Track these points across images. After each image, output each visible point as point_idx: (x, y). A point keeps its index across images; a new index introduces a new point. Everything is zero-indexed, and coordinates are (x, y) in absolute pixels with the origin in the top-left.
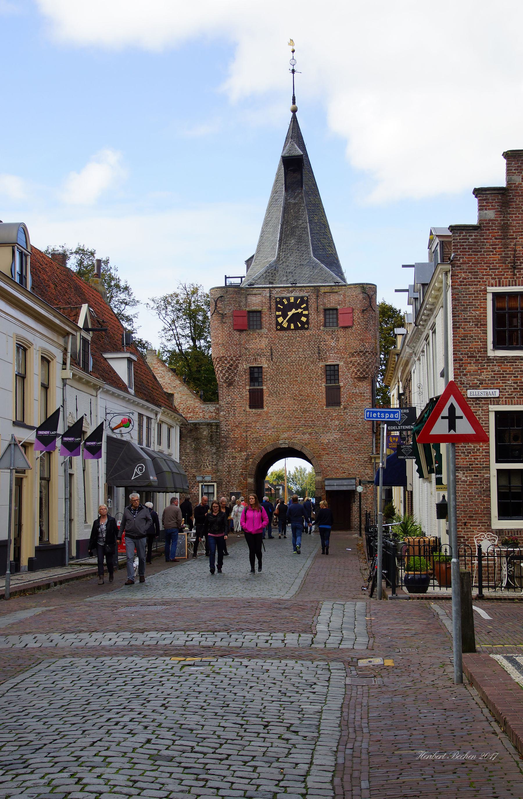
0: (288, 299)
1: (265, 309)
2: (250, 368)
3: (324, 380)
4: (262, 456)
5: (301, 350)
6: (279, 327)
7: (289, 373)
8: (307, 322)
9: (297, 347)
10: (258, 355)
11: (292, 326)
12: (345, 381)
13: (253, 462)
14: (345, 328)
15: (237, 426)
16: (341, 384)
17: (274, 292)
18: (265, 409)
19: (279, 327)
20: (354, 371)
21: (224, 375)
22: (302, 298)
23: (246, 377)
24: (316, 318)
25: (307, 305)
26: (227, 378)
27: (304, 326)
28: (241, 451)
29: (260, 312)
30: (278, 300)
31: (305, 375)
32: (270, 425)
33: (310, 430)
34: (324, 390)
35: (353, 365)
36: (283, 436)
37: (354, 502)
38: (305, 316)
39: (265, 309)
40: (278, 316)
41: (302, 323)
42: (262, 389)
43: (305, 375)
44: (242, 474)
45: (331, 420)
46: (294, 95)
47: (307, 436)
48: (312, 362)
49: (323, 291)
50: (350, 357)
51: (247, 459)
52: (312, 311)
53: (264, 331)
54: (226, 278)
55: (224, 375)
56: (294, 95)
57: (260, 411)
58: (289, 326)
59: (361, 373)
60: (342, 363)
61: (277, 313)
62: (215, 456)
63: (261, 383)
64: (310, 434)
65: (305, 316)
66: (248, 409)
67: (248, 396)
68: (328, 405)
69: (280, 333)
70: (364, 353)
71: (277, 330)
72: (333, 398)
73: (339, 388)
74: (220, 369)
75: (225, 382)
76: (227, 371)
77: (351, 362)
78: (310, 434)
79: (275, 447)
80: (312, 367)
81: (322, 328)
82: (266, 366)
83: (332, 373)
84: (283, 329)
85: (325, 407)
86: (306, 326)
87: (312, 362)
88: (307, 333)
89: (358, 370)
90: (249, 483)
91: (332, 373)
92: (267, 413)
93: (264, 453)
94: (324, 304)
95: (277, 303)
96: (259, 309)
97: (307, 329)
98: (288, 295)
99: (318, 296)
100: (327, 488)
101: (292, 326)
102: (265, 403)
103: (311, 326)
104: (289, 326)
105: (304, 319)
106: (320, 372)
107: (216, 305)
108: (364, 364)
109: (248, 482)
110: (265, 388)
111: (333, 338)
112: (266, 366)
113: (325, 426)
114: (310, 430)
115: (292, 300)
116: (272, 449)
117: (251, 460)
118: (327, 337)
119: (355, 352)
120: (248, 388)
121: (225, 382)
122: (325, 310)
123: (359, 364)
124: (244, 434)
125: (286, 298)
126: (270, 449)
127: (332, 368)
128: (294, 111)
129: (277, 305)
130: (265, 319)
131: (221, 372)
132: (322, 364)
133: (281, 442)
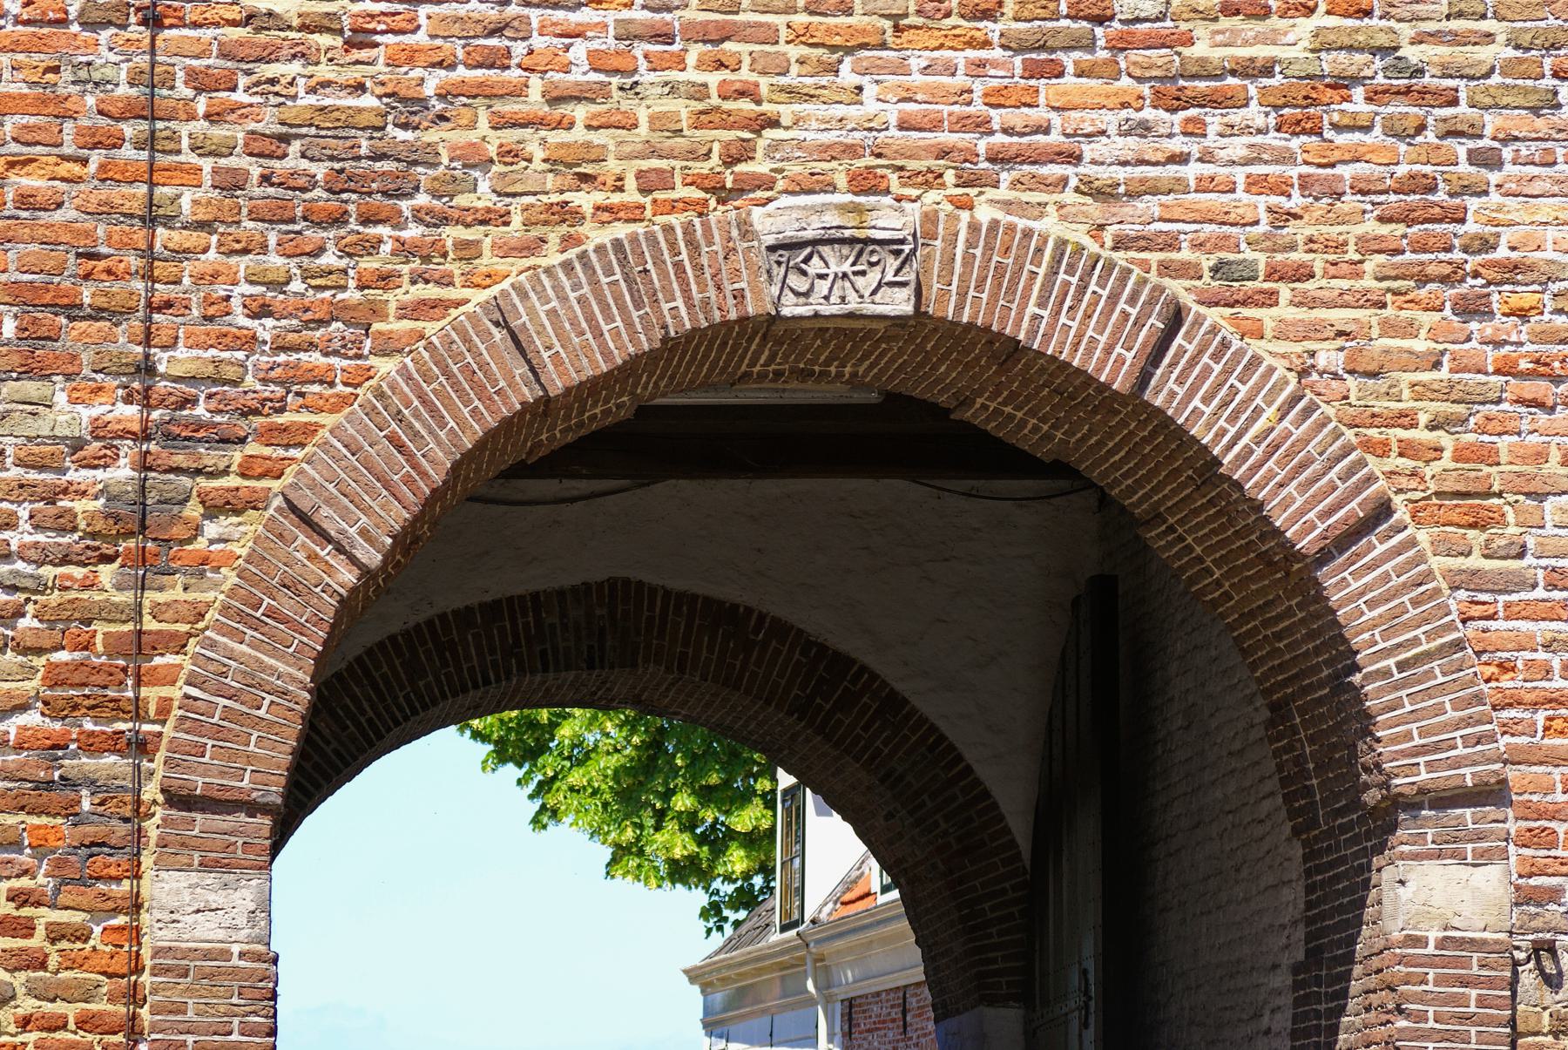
4: (437, 460)
13: (256, 566)
36: (811, 124)
47: (1238, 138)
51: (140, 532)
64: (1304, 106)
78: (1304, 106)
79: (678, 314)
90: (175, 964)
93: (468, 424)
109: (155, 934)
116: (621, 338)
117: (235, 535)
124: (113, 57)
126: (581, 339)
133: (775, 219)
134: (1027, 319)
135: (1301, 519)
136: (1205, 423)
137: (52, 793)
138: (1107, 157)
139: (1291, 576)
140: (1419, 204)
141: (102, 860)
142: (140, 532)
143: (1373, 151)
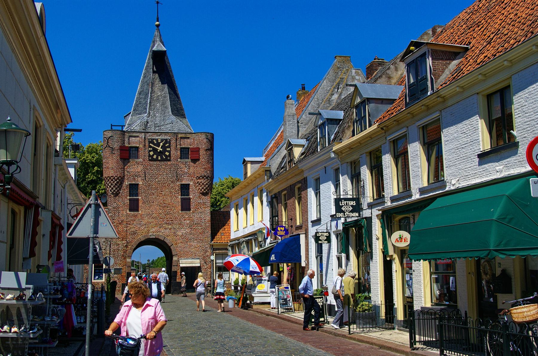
0: (157, 140)
1: (141, 146)
2: (130, 184)
3: (180, 193)
6: (150, 158)
7: (156, 189)
8: (170, 155)
9: (162, 172)
10: (136, 176)
11: (159, 158)
12: (193, 195)
15: (120, 224)
16: (191, 197)
17: (148, 135)
18: (140, 212)
19: (150, 158)
21: (112, 189)
22: (166, 140)
23: (127, 191)
24: (175, 153)
25: (170, 144)
26: (114, 191)
27: (168, 159)
28: (122, 240)
29: (138, 148)
30: (150, 140)
31: (167, 190)
32: (143, 223)
33: (170, 227)
34: (180, 200)
35: (199, 184)
36: (152, 231)
38: (168, 151)
39: (141, 146)
40: (150, 151)
41: (166, 156)
42: (138, 200)
43: (167, 190)
44: (123, 256)
45: (185, 220)
48: (172, 182)
49: (180, 136)
51: (126, 246)
52: (173, 148)
53: (141, 160)
54: (112, 126)
55: (112, 189)
57: (136, 213)
58: (157, 157)
59: (205, 190)
60: (192, 183)
61: (150, 149)
62: (104, 244)
63: (137, 195)
64: (170, 229)
65: (168, 151)
66: (128, 212)
67: (128, 203)
68: (182, 210)
69: (152, 163)
71: (150, 160)
72: (186, 205)
73: (190, 199)
74: (110, 184)
75: (113, 193)
76: (114, 186)
78: (170, 229)
80: (172, 185)
81: (179, 160)
82: (141, 183)
83: (185, 189)
84: (153, 160)
85: (180, 212)
86: (169, 158)
87: (172, 182)
88: (169, 163)
89: (203, 188)
91: (185, 189)
92: (141, 215)
93: (138, 242)
94: (180, 145)
95: (150, 142)
96: (138, 146)
97: (170, 160)
98: (157, 138)
99: (176, 139)
100: (181, 265)
101: (159, 158)
102: (140, 208)
103: (172, 158)
104: (157, 157)
105: (167, 154)
106: (177, 188)
107: (108, 142)
110: (140, 198)
111: (186, 167)
112: (141, 183)
113: (180, 224)
114: (170, 227)
115: (159, 141)
116: (144, 239)
118: (182, 166)
120: (128, 197)
121: (113, 193)
122: (181, 148)
123: (203, 184)
124: (125, 229)
125: (156, 139)
129: (149, 144)
130: (141, 152)
131: (110, 187)
132: (178, 183)
133: (150, 234)
134: (159, 238)
136: (167, 242)
137: (123, 256)
138: (163, 231)
139: (169, 247)
140: (174, 233)
141: (125, 258)
142: (126, 246)
143: (173, 231)
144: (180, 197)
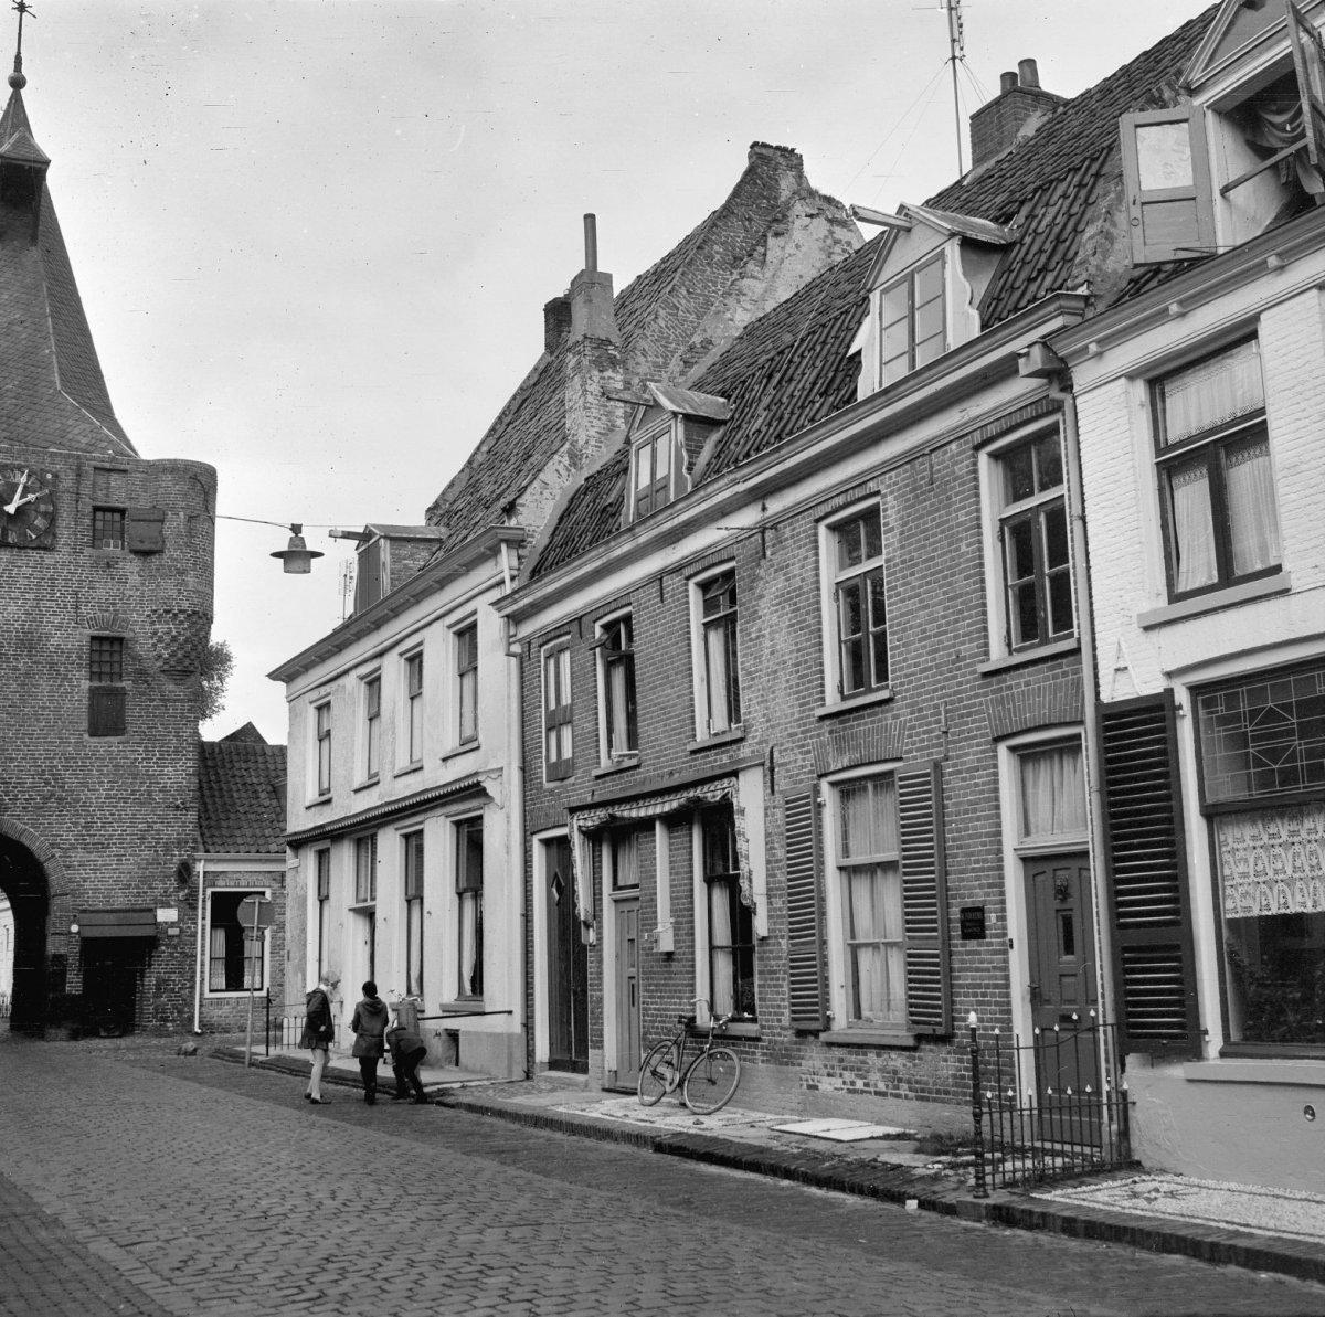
5: (32, 596)
14: (145, 554)
20: (160, 656)
37: (150, 965)
46: (19, 53)
50: (153, 623)
56: (19, 53)
70: (189, 615)
77: (155, 633)
88: (49, 559)
108: (186, 641)
119: (167, 612)
122: (96, 509)
123: (174, 639)
127: (106, 647)
128: (17, 83)
135: (42, 859)
144: (86, 684)
